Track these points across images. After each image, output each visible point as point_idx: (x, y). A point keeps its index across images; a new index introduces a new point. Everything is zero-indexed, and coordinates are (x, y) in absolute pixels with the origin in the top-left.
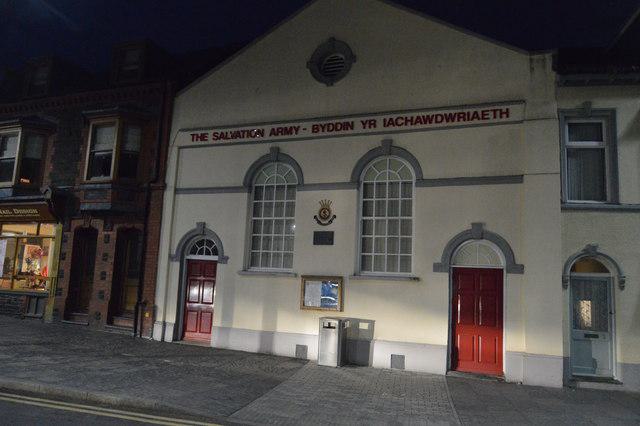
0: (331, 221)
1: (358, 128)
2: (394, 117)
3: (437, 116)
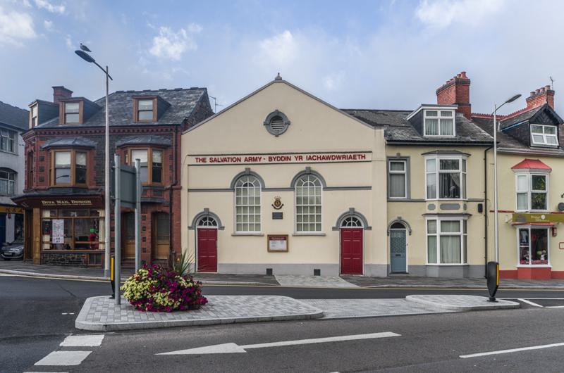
0: (281, 208)
1: (293, 160)
2: (312, 155)
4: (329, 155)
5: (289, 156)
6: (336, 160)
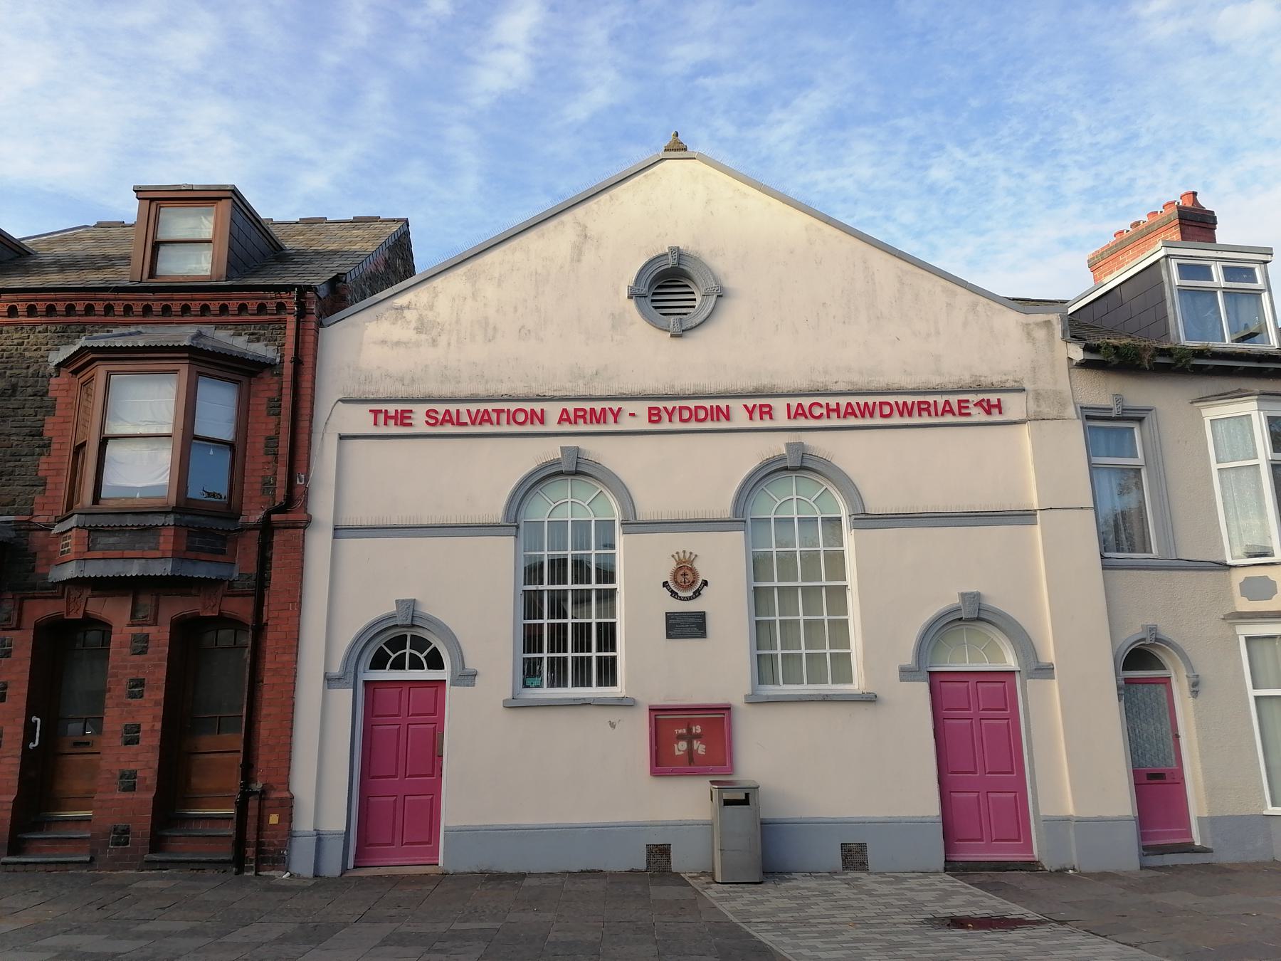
0: (697, 593)
1: (740, 418)
2: (806, 402)
3: (681, 408)
4: (870, 400)
5: (722, 404)
6: (896, 420)
